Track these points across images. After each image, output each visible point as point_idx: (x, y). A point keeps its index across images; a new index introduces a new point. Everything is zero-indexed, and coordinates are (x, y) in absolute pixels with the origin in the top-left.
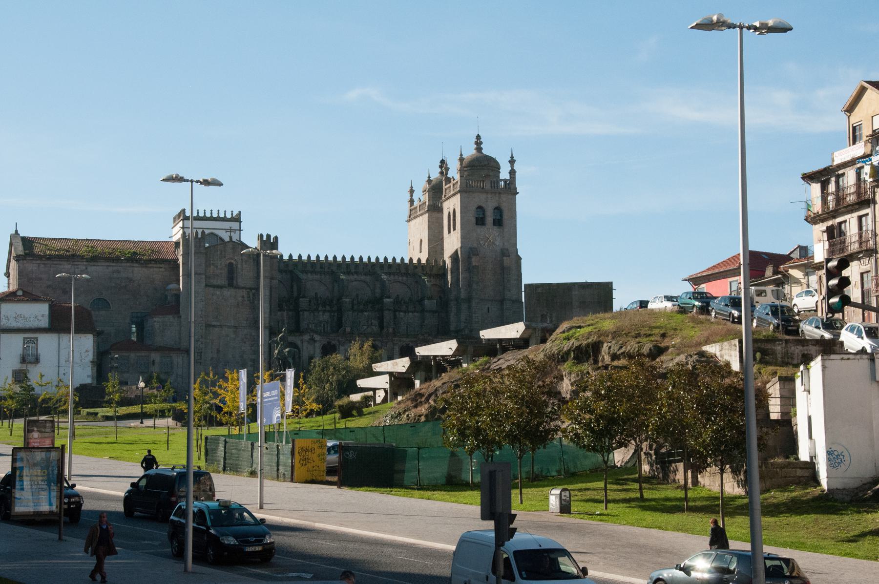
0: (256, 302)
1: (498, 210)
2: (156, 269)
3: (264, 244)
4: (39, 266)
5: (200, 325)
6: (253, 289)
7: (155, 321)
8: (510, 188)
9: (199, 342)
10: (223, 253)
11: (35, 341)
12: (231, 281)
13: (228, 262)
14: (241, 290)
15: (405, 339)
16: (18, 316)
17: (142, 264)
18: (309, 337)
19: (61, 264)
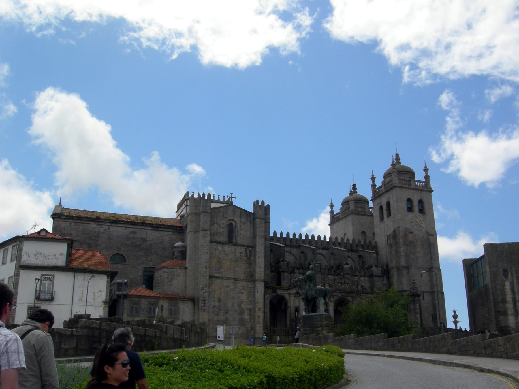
0: (252, 258)
1: (421, 202)
2: (165, 233)
3: (260, 208)
4: (70, 224)
5: (205, 275)
6: (250, 247)
7: (164, 272)
8: (427, 188)
9: (203, 291)
10: (225, 215)
11: (51, 279)
12: (231, 240)
13: (230, 222)
14: (239, 247)
16: (38, 254)
17: (154, 227)
18: (295, 291)
19: (88, 223)
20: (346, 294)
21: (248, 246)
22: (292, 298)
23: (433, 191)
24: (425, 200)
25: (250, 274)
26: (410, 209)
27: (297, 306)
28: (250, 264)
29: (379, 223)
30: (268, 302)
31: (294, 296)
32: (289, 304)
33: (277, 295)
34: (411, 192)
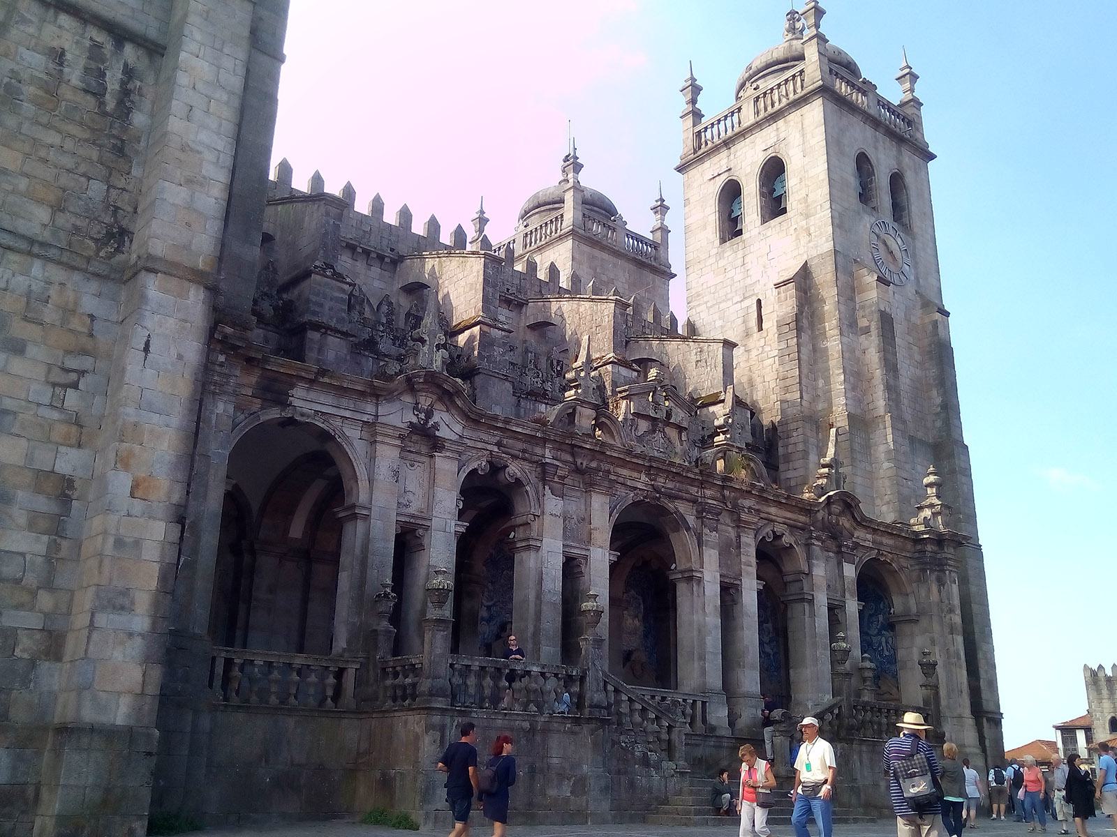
0: (139, 119)
1: (897, 181)
15: (773, 510)
20: (670, 485)
21: (120, 35)
22: (388, 455)
23: (932, 157)
24: (909, 178)
25: (108, 219)
26: (865, 195)
27: (413, 516)
28: (120, 150)
29: (715, 251)
30: (219, 450)
31: (398, 442)
32: (363, 497)
33: (291, 421)
34: (869, 131)
